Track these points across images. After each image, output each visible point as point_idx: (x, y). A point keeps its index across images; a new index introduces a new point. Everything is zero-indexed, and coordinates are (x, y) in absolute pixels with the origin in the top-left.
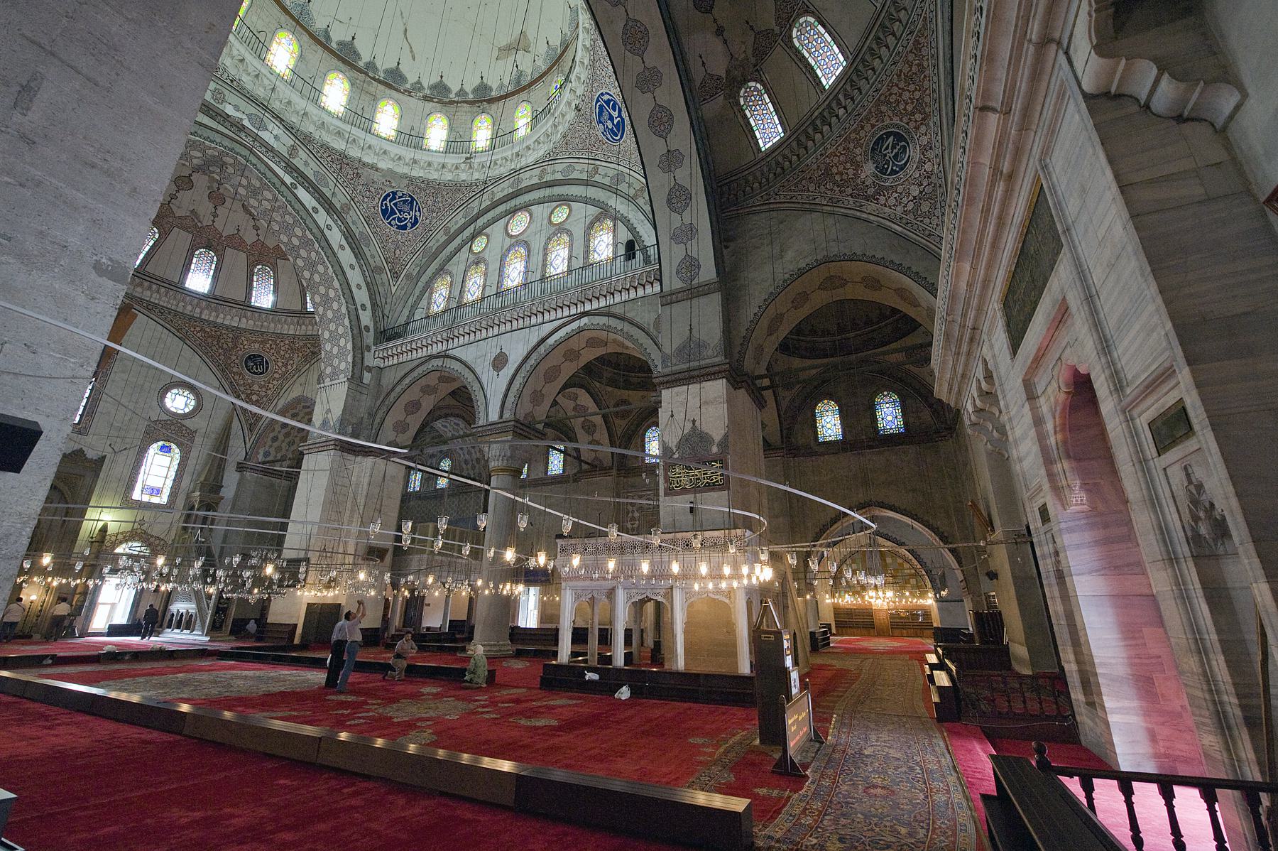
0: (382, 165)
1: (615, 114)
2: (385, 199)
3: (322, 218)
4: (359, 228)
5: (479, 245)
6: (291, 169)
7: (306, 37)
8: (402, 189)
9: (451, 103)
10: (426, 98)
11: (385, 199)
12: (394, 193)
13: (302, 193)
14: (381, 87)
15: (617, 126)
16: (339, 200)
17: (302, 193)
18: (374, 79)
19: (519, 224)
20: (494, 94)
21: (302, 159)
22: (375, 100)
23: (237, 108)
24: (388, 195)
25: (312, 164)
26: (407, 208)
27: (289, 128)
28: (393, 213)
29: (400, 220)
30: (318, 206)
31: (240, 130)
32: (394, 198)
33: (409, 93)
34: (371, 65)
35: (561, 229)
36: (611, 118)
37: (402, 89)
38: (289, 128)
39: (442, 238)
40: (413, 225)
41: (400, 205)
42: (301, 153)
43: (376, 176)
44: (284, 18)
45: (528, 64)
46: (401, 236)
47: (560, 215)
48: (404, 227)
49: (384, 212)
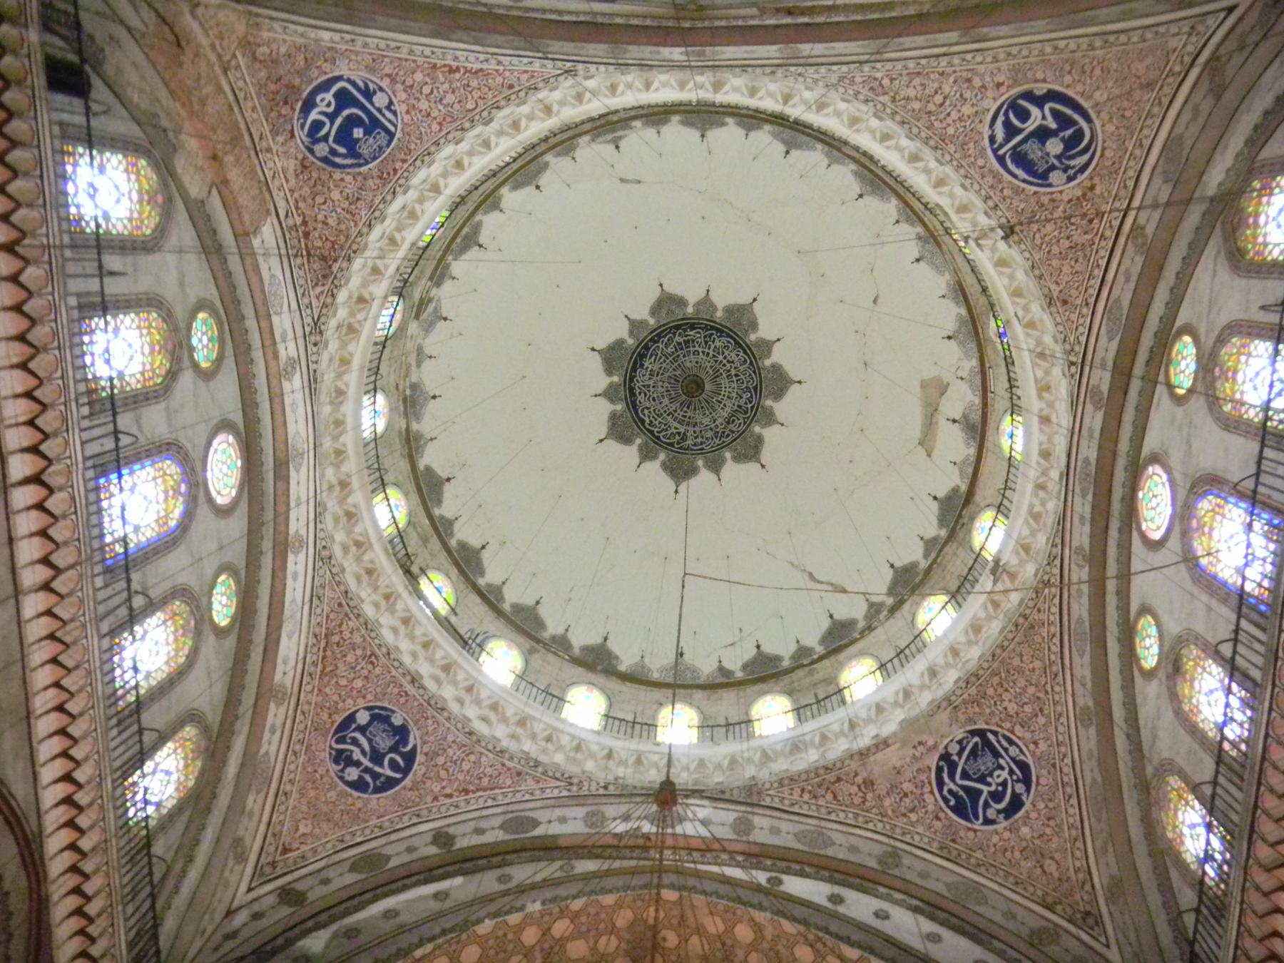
0: (889, 728)
1: (1037, 117)
2: (940, 784)
3: (860, 906)
4: (941, 875)
5: (1149, 652)
6: (757, 856)
7: (698, 695)
8: (951, 733)
9: (928, 571)
10: (894, 610)
11: (940, 784)
12: (946, 757)
13: (795, 886)
14: (826, 663)
15: (1063, 121)
16: (868, 852)
17: (795, 886)
18: (813, 662)
19: (1156, 504)
20: (964, 488)
21: (765, 829)
22: (832, 680)
23: (626, 818)
24: (939, 770)
25: (785, 826)
26: (986, 762)
27: (718, 797)
28: (974, 794)
29: (997, 796)
30: (837, 889)
31: (645, 848)
32: (952, 767)
33: (870, 628)
34: (802, 651)
35: (1209, 365)
36: (1042, 134)
37: (856, 635)
38: (718, 797)
39: (1089, 738)
40: (1027, 781)
41: (974, 771)
42: (757, 821)
43: (892, 757)
44: (657, 694)
45: (961, 399)
46: (1027, 826)
47: (1184, 365)
48: (1016, 804)
49: (960, 810)
